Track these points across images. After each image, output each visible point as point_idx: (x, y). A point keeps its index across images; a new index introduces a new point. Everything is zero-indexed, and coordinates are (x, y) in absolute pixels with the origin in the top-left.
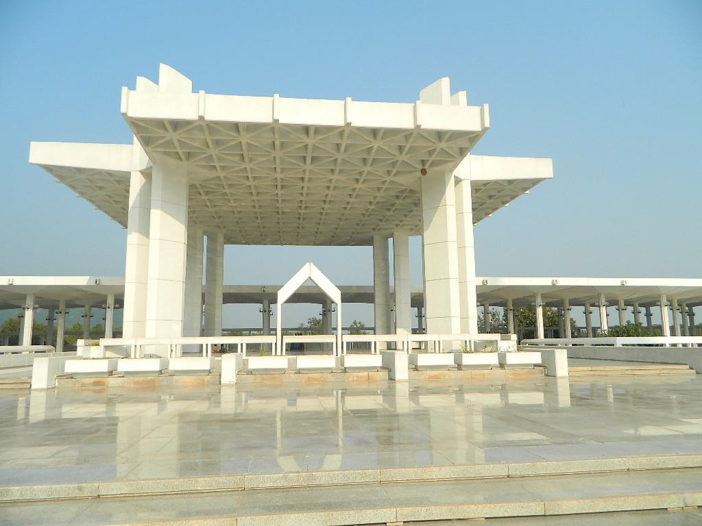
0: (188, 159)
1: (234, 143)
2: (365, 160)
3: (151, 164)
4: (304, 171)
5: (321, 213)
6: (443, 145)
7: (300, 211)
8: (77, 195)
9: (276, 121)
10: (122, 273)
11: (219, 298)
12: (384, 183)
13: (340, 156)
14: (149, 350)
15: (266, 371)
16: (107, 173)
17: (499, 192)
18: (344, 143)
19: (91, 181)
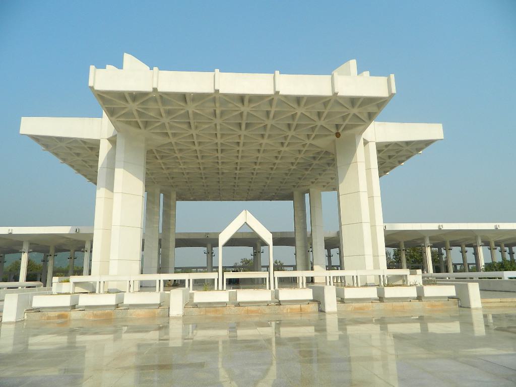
0: (145, 127)
1: (182, 112)
2: (289, 126)
3: (116, 133)
4: (240, 136)
5: (253, 173)
6: (355, 111)
7: (236, 172)
8: (61, 161)
9: (217, 91)
10: (91, 223)
11: (172, 243)
12: (304, 146)
13: (269, 122)
14: (112, 286)
15: (210, 305)
16: (82, 141)
17: (397, 152)
18: (273, 110)
19: (70, 149)
